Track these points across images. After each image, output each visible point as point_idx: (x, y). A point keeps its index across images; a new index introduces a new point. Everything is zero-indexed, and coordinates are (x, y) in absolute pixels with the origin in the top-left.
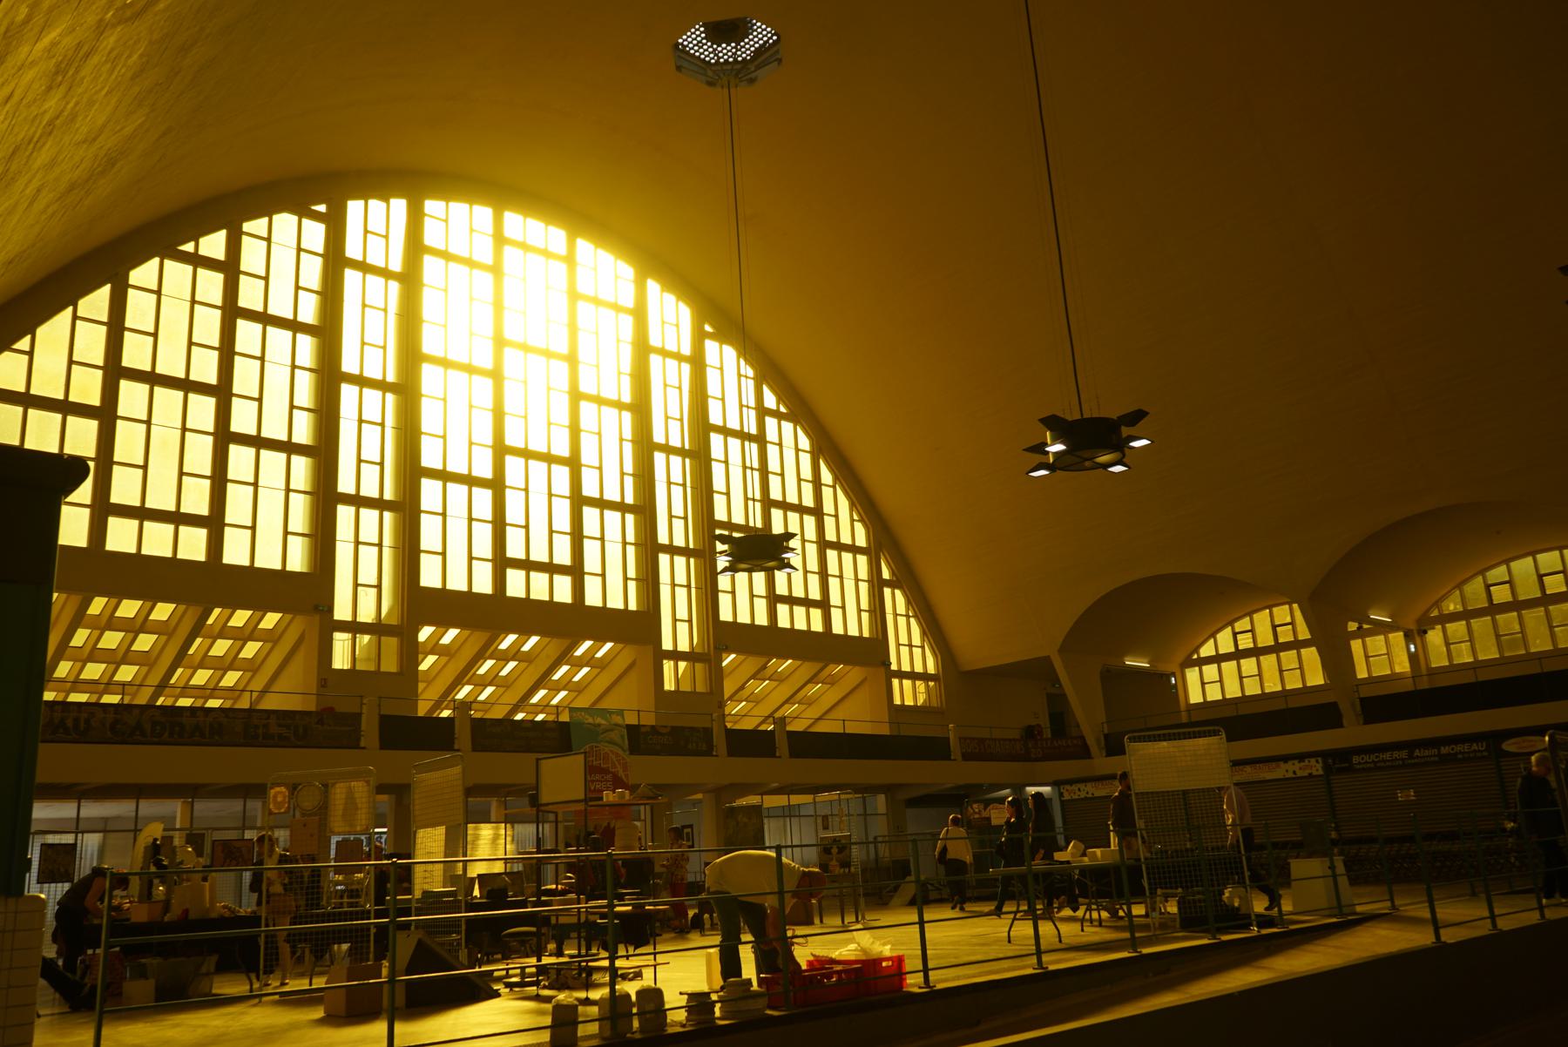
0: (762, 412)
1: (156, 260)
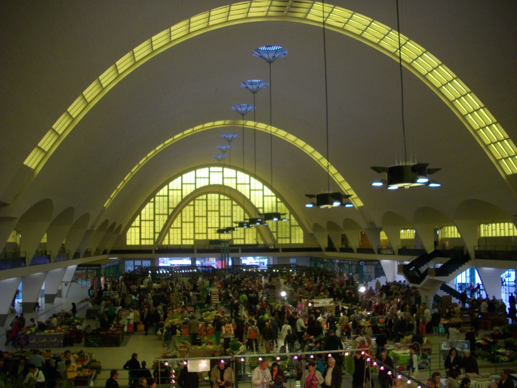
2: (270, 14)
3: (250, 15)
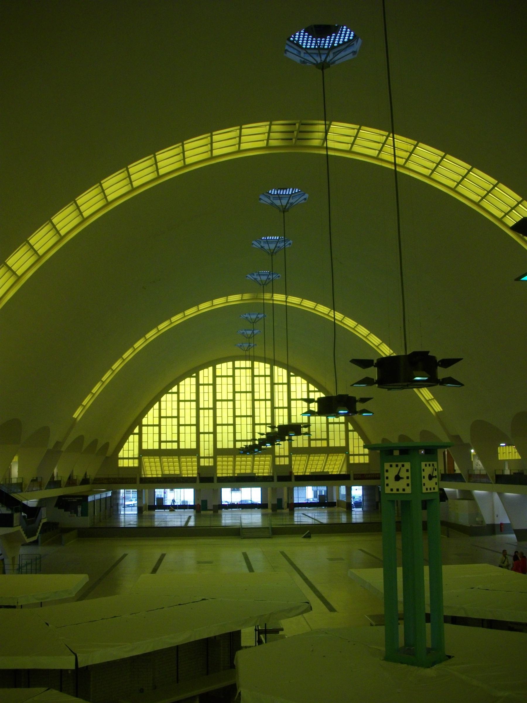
0: (309, 391)
1: (165, 395)
2: (272, 143)
3: (244, 146)
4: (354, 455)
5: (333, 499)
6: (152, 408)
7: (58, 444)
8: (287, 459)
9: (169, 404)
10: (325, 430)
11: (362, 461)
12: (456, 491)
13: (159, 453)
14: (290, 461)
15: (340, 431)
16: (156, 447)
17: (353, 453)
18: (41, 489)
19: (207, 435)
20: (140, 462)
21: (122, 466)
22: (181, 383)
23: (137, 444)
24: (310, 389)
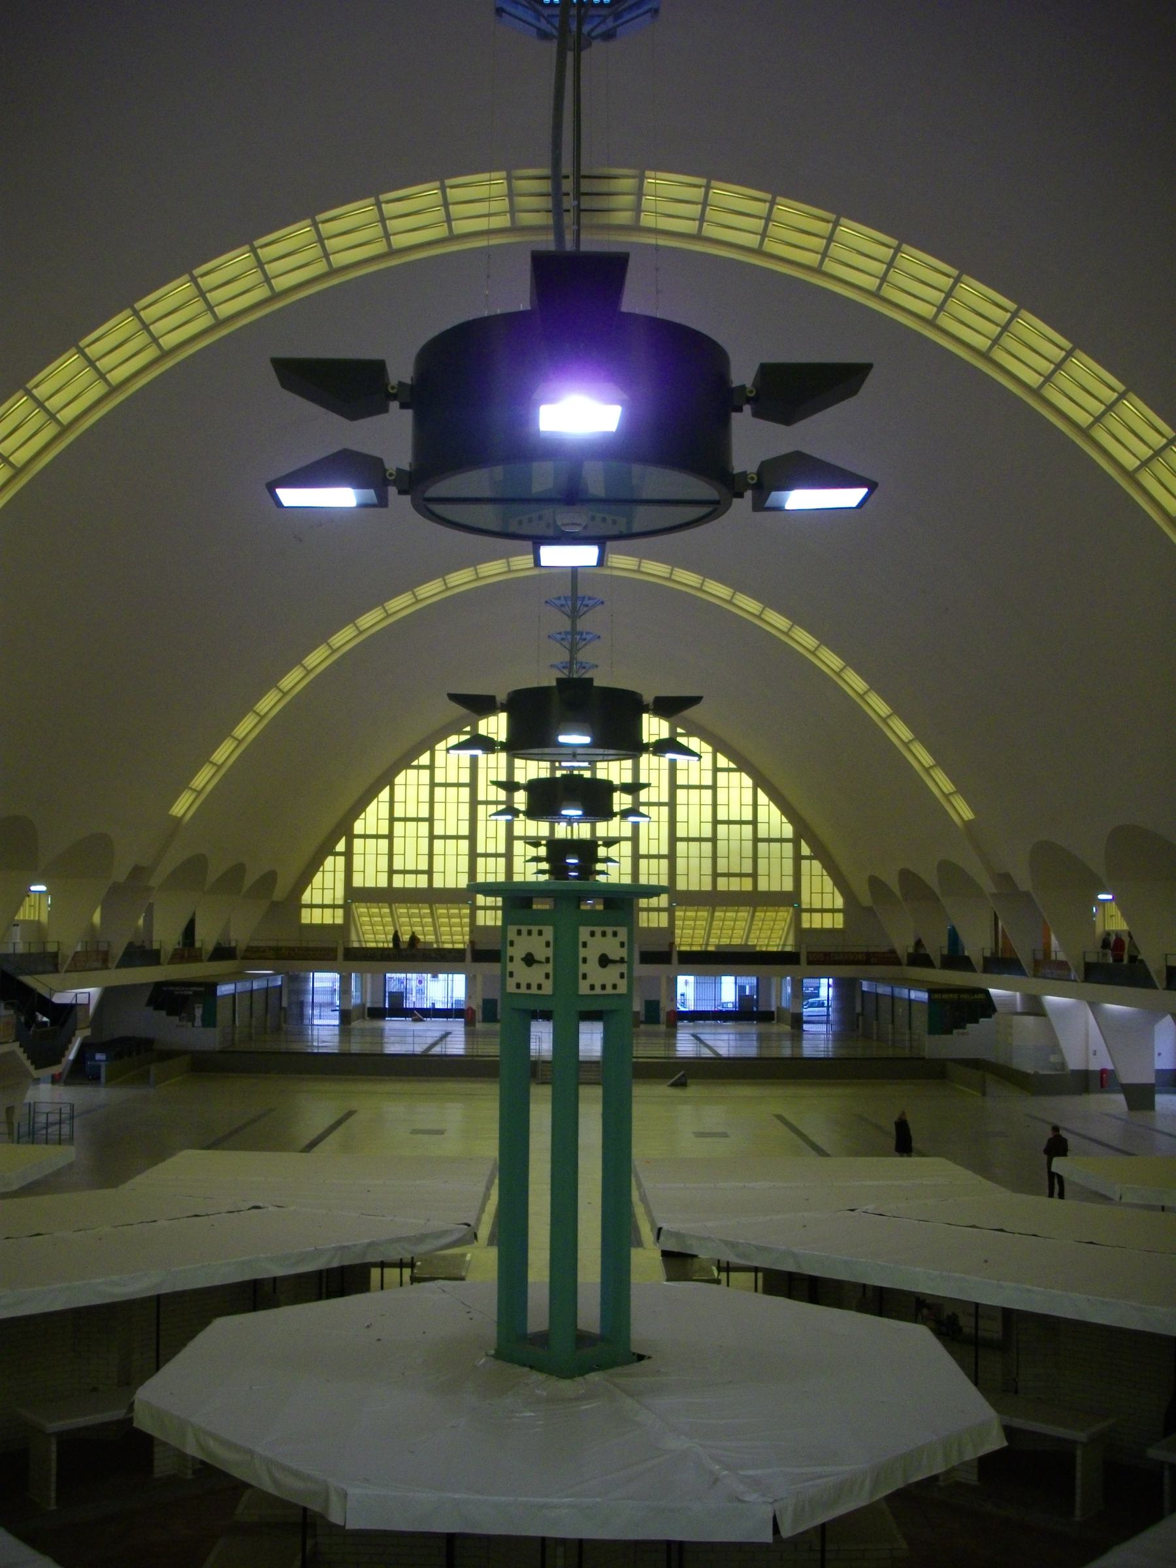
0: (716, 770)
4: (811, 911)
5: (770, 1006)
6: (376, 799)
7: (138, 872)
8: (664, 916)
9: (412, 791)
10: (750, 854)
11: (828, 924)
12: (1015, 996)
13: (388, 896)
14: (672, 919)
15: (782, 858)
16: (383, 882)
17: (809, 907)
18: (107, 968)
19: (491, 860)
20: (348, 915)
21: (309, 922)
22: (438, 747)
23: (341, 876)
24: (719, 765)
